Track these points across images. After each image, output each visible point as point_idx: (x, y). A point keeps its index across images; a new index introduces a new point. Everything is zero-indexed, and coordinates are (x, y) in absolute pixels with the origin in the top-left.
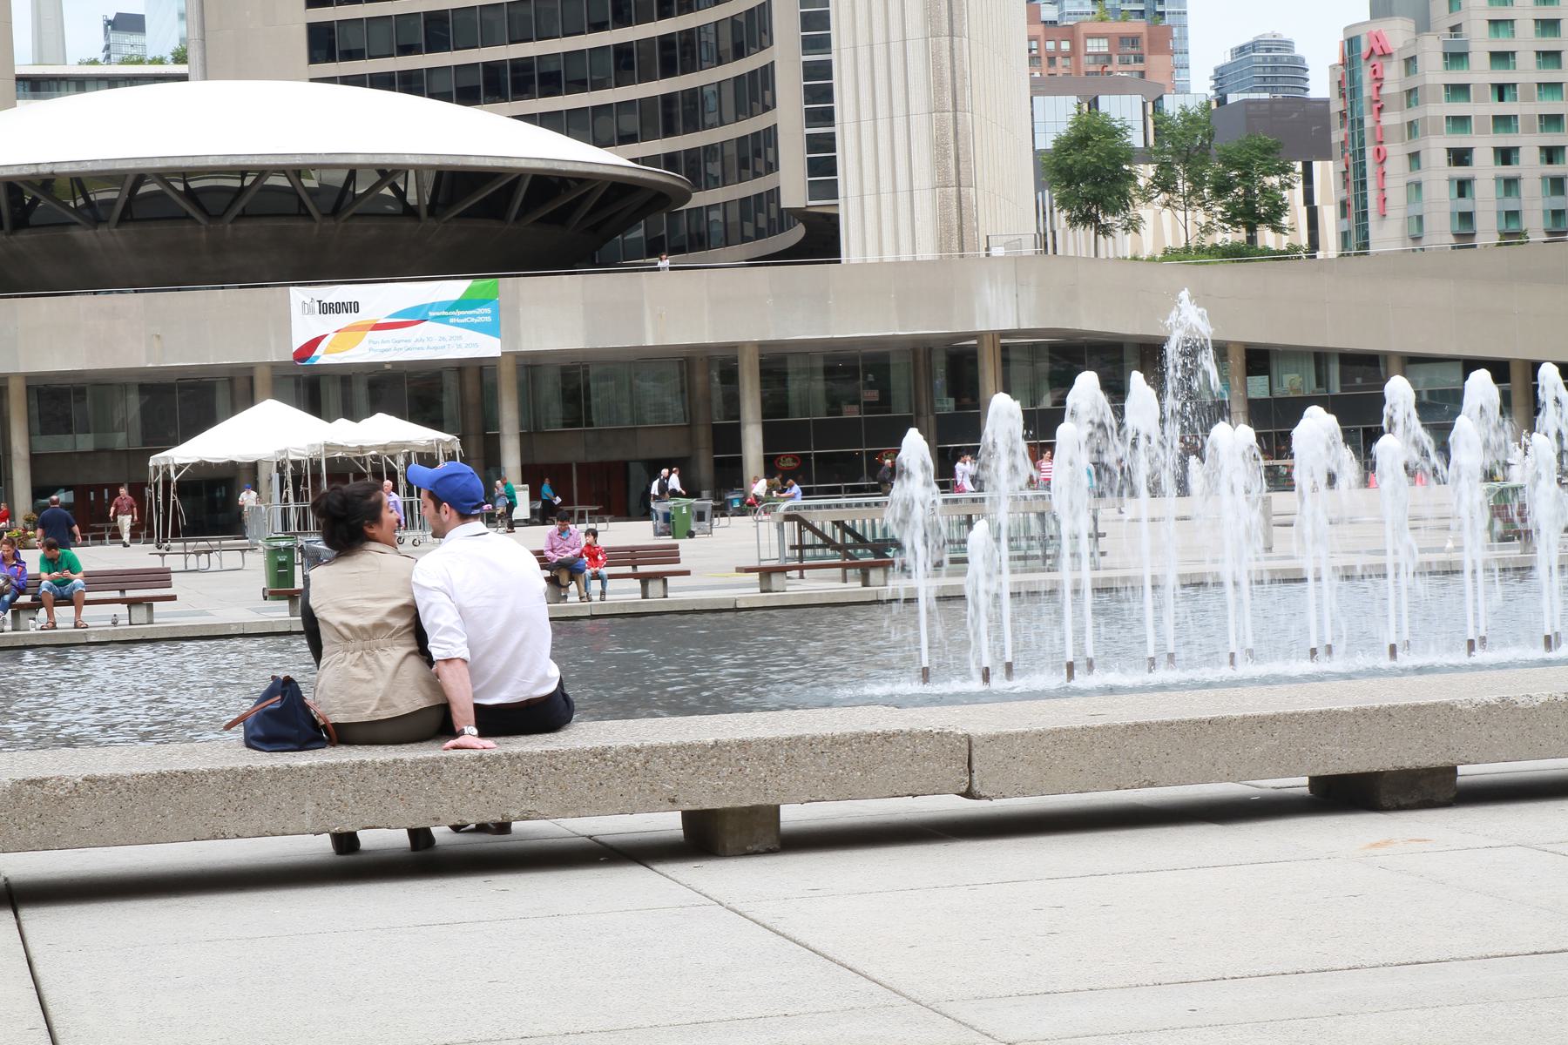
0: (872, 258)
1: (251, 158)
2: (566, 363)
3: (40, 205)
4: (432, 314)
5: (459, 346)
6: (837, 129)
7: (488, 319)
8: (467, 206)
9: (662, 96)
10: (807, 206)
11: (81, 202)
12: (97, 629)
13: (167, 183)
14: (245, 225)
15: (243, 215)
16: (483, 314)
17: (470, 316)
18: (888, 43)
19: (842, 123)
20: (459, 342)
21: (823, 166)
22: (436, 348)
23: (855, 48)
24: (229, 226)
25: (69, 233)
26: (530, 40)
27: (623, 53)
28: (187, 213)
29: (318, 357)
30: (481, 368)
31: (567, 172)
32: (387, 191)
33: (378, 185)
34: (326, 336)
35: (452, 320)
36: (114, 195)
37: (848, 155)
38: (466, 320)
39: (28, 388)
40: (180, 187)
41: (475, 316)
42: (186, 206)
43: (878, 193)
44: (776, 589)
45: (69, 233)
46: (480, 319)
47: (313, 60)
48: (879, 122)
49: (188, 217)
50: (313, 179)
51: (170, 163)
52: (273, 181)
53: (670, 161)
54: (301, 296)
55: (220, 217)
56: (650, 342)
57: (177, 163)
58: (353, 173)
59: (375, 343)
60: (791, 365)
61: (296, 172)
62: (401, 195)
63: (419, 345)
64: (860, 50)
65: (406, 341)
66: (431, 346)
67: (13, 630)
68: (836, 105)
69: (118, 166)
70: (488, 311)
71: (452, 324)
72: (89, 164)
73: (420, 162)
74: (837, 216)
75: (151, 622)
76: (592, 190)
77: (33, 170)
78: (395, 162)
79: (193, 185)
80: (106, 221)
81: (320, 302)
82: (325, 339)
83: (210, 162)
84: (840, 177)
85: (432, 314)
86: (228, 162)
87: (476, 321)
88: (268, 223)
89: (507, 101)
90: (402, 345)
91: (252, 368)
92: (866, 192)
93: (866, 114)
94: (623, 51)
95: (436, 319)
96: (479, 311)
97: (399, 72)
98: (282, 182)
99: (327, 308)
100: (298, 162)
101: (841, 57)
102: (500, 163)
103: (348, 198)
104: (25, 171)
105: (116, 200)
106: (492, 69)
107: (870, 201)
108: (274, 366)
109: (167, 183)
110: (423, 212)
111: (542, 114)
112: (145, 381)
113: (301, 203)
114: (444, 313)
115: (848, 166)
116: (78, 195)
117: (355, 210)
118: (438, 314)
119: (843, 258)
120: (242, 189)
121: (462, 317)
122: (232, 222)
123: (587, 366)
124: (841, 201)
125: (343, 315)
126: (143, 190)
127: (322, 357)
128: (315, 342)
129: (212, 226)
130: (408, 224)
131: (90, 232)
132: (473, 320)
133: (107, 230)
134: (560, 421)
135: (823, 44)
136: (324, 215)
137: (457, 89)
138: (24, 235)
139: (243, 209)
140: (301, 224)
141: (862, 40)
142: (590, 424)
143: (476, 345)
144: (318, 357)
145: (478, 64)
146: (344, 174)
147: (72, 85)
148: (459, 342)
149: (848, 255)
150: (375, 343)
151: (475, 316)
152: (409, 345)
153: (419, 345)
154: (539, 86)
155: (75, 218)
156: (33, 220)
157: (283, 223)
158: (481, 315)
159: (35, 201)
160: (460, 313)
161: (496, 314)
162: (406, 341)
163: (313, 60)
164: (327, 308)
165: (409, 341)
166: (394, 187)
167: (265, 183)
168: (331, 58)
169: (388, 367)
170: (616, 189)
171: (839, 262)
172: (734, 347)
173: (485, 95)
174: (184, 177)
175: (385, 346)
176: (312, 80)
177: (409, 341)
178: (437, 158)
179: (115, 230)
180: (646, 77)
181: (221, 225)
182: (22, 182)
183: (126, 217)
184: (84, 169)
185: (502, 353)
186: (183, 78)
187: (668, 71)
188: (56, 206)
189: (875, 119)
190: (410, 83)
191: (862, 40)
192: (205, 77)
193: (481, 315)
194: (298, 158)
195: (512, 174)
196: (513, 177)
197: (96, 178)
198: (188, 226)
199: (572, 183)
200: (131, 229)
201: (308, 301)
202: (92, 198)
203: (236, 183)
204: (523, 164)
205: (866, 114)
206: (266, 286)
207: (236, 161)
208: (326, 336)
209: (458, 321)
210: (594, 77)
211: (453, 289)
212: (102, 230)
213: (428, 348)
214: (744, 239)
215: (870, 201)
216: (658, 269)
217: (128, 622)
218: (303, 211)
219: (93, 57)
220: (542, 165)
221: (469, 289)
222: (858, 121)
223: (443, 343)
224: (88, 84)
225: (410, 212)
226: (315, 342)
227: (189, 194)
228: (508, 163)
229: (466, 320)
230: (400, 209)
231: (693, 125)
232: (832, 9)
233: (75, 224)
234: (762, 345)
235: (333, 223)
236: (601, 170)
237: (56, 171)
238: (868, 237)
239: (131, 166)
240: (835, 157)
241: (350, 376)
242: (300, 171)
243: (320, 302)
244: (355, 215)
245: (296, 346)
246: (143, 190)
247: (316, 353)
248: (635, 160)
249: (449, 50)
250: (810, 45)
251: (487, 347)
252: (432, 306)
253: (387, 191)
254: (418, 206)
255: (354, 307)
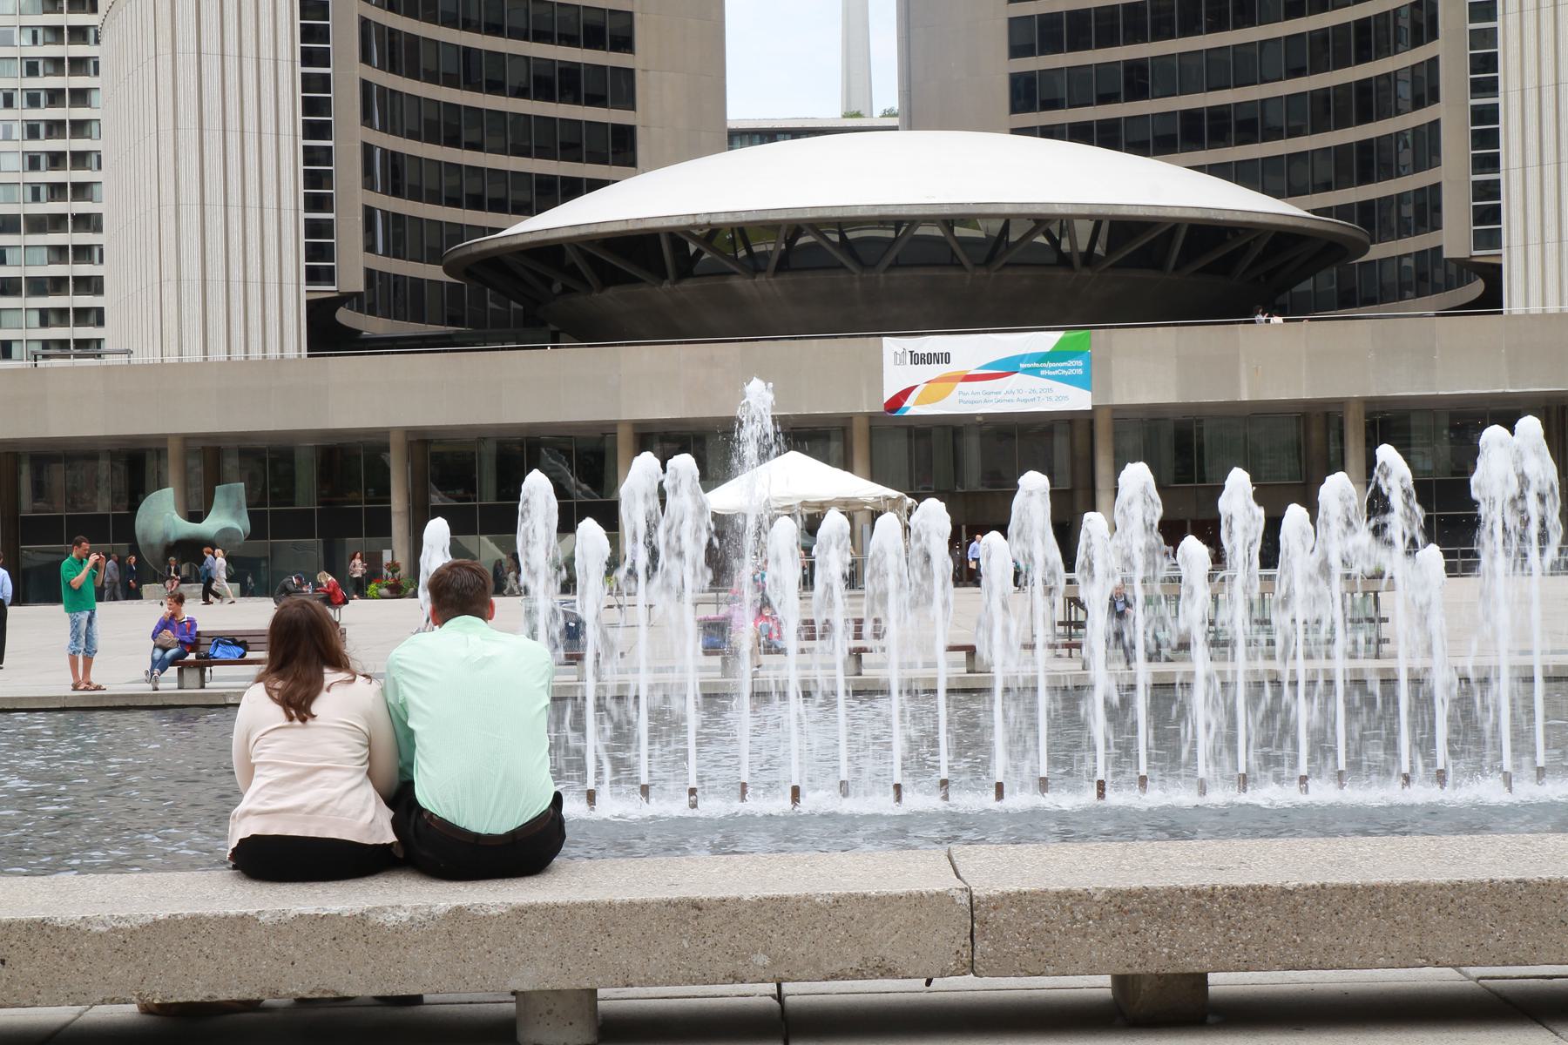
0: (1535, 308)
1: (899, 208)
2: (327, 443)
3: (703, 258)
4: (1022, 366)
5: (1050, 399)
6: (1502, 176)
7: (1080, 371)
8: (1121, 256)
9: (1357, 142)
10: (1471, 257)
11: (742, 253)
12: (236, 691)
13: (822, 235)
14: (897, 274)
15: (896, 265)
16: (1075, 366)
17: (1063, 368)
18: (1540, 88)
19: (1507, 169)
20: (1050, 395)
21: (1488, 215)
22: (1026, 401)
23: (1523, 90)
24: (882, 275)
25: (727, 282)
26: (1227, 87)
27: (1321, 98)
28: (842, 263)
29: (908, 408)
30: (1327, 414)
31: (1223, 221)
32: (1041, 239)
33: (1032, 232)
34: (916, 386)
35: (1042, 372)
36: (771, 247)
37: (1513, 204)
38: (1057, 372)
39: (635, 434)
40: (835, 238)
41: (1066, 368)
42: (840, 257)
43: (1543, 242)
44: (979, 670)
45: (727, 282)
46: (1071, 372)
47: (1014, 110)
48: (1546, 168)
49: (842, 266)
50: (979, 229)
51: (821, 214)
52: (922, 231)
53: (1341, 211)
54: (893, 346)
55: (873, 266)
56: (1245, 397)
57: (827, 213)
58: (1008, 220)
59: (965, 394)
60: (1413, 423)
61: (949, 221)
62: (1056, 244)
63: (1009, 397)
64: (1527, 92)
65: (996, 393)
66: (1022, 397)
67: (179, 688)
68: (1502, 150)
69: (771, 217)
70: (1080, 363)
71: (1044, 377)
72: (743, 214)
73: (1070, 212)
74: (1499, 267)
75: (203, 687)
76: (1254, 240)
77: (691, 221)
78: (1044, 212)
79: (851, 235)
80: (764, 271)
81: (911, 352)
82: (914, 392)
83: (859, 213)
84: (1504, 226)
85: (1022, 366)
86: (877, 213)
87: (1067, 373)
88: (920, 272)
89: (1203, 149)
90: (992, 397)
91: (851, 418)
92: (1531, 241)
93: (1533, 158)
94: (1322, 96)
95: (1027, 371)
96: (1071, 363)
97: (1098, 121)
98: (937, 232)
99: (918, 359)
100: (945, 212)
101: (1509, 100)
102: (1152, 212)
103: (1003, 247)
104: (683, 222)
105: (771, 252)
106: (1190, 116)
107: (1534, 251)
108: (871, 417)
109: (822, 235)
110: (1077, 261)
111: (1211, 166)
112: (248, 444)
113: (953, 253)
114: (1037, 365)
115: (1513, 215)
116: (739, 243)
117: (1004, 261)
118: (1029, 366)
119: (1505, 309)
120: (891, 243)
121: (1053, 369)
122: (885, 272)
123: (1202, 421)
124: (1504, 251)
125: (934, 366)
126: (802, 241)
127: (912, 408)
128: (906, 393)
129: (865, 275)
130: (1061, 273)
131: (749, 281)
132: (1064, 372)
133: (764, 279)
134: (1287, 474)
135: (1491, 87)
136: (976, 265)
137: (1155, 138)
138: (687, 284)
139: (897, 258)
140: (953, 273)
141: (1531, 83)
142: (1202, 480)
143: (1066, 398)
144: (908, 408)
145: (1175, 112)
146: (997, 226)
147: (789, 136)
148: (1050, 395)
149: (1510, 306)
150: (965, 394)
151: (1066, 368)
152: (999, 397)
153: (1009, 397)
154: (1236, 133)
155: (734, 268)
156: (696, 270)
157: (936, 272)
158: (1072, 368)
159: (699, 253)
160: (1051, 365)
161: (1088, 367)
162: (996, 393)
163: (1014, 110)
164: (918, 359)
165: (1000, 393)
166: (1048, 235)
167: (916, 233)
168: (1029, 108)
169: (979, 419)
170: (1280, 238)
171: (1501, 313)
172: (1342, 403)
173: (1209, 139)
174: (840, 229)
175: (976, 398)
176: (1015, 131)
177: (1000, 393)
178: (1087, 207)
179: (772, 279)
180: (1342, 123)
181: (874, 275)
182: (683, 232)
183: (784, 264)
184: (738, 220)
185: (1093, 406)
186: (895, 128)
187: (1365, 117)
188: (721, 260)
189: (1541, 164)
190: (1080, 133)
191: (1531, 83)
192: (910, 127)
193: (1072, 368)
194: (905, 208)
195: (1166, 224)
196: (1167, 227)
197: (763, 227)
198: (842, 276)
199: (1241, 232)
200: (787, 277)
201: (900, 351)
202: (756, 249)
203: (891, 234)
204: (1177, 213)
205: (1533, 158)
206: (836, 337)
207: (884, 212)
208: (916, 386)
209: (1050, 373)
210: (1292, 124)
211: (1045, 340)
212: (760, 279)
213: (1018, 400)
214: (1436, 289)
215: (1534, 251)
216: (1254, 322)
217: (176, 685)
218: (956, 261)
219: (856, 110)
220: (1197, 214)
221: (1061, 341)
222: (1524, 167)
223: (1031, 396)
224: (778, 136)
225: (1065, 260)
226: (906, 393)
227: (845, 244)
228: (1161, 213)
229: (1057, 372)
230: (1053, 258)
231: (1390, 172)
232: (1500, 50)
233: (734, 273)
234: (1368, 402)
235: (985, 273)
236: (1261, 219)
237: (712, 221)
238: (1531, 289)
239: (783, 216)
240: (1499, 206)
241: (961, 427)
242: (953, 221)
243: (911, 352)
244: (1006, 265)
245: (888, 395)
246: (802, 241)
247: (906, 404)
248: (1314, 212)
249: (1148, 98)
250: (1479, 88)
251: (1078, 400)
252: (1022, 358)
253: (1041, 239)
254: (1070, 254)
255: (945, 358)
